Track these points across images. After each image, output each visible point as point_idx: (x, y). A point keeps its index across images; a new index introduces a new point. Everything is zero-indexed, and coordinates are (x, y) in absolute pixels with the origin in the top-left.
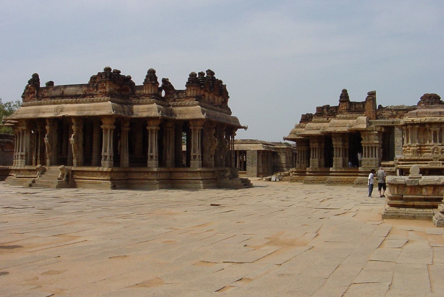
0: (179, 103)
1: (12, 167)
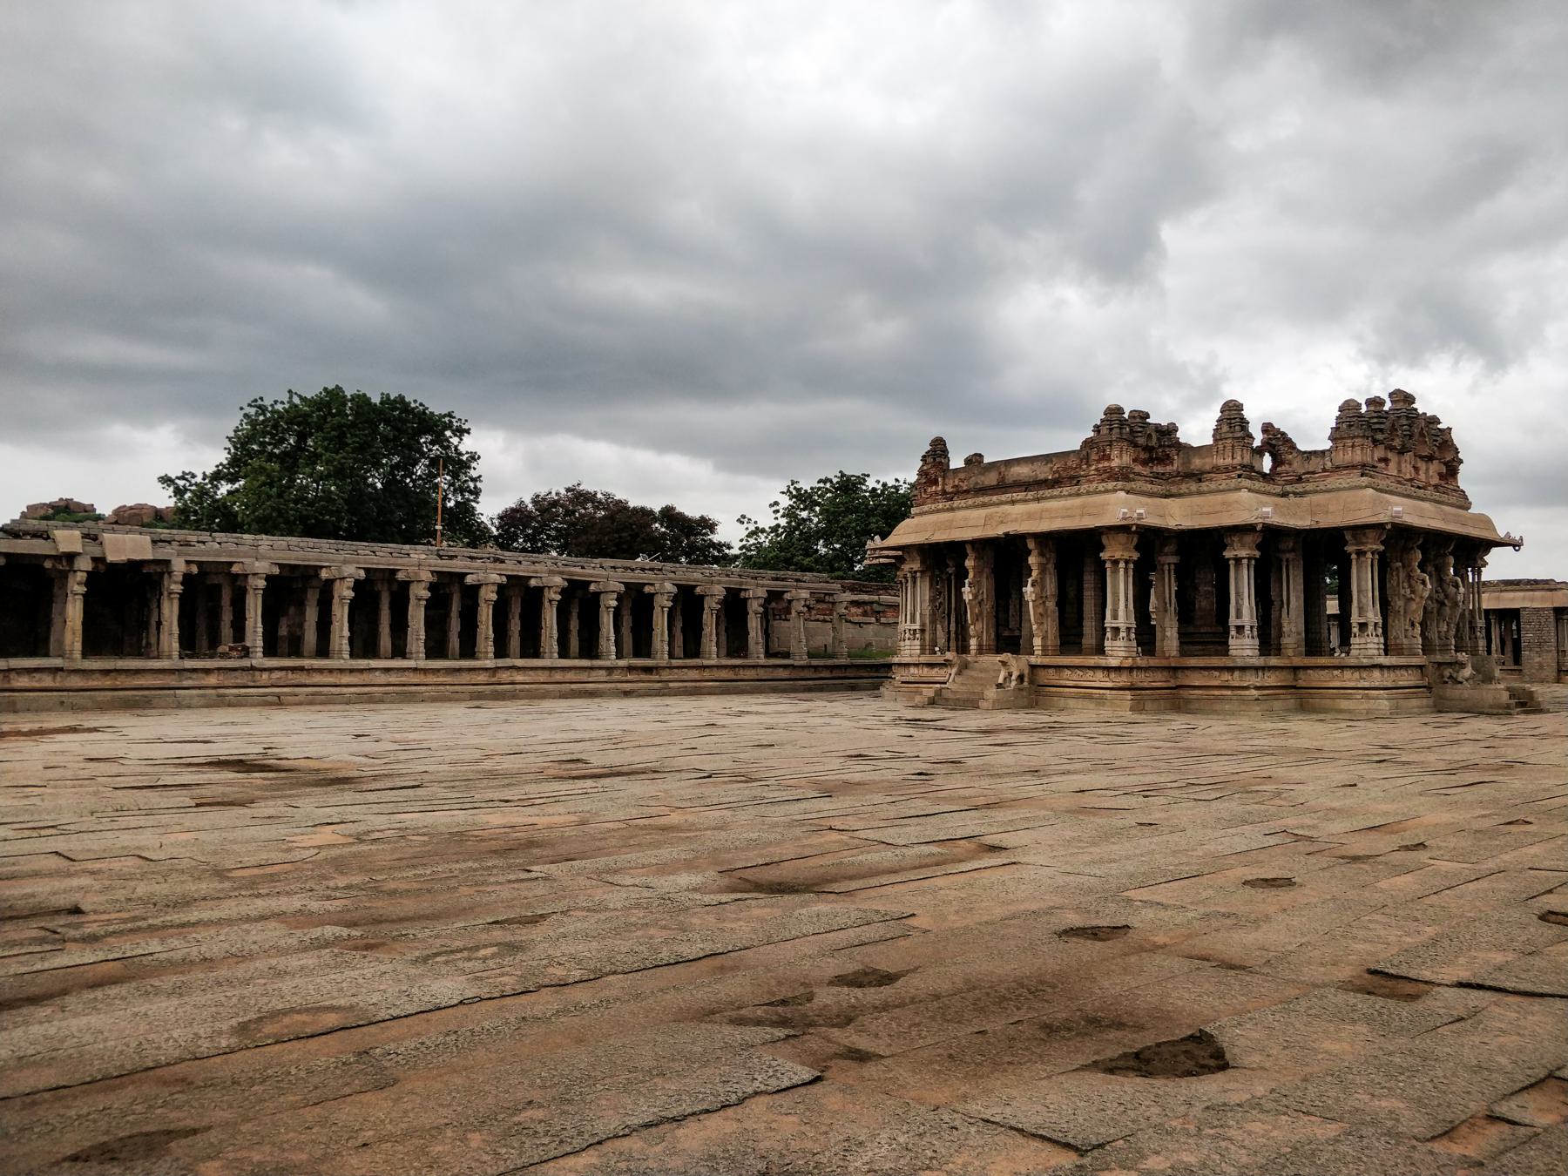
0: (1310, 487)
1: (896, 660)
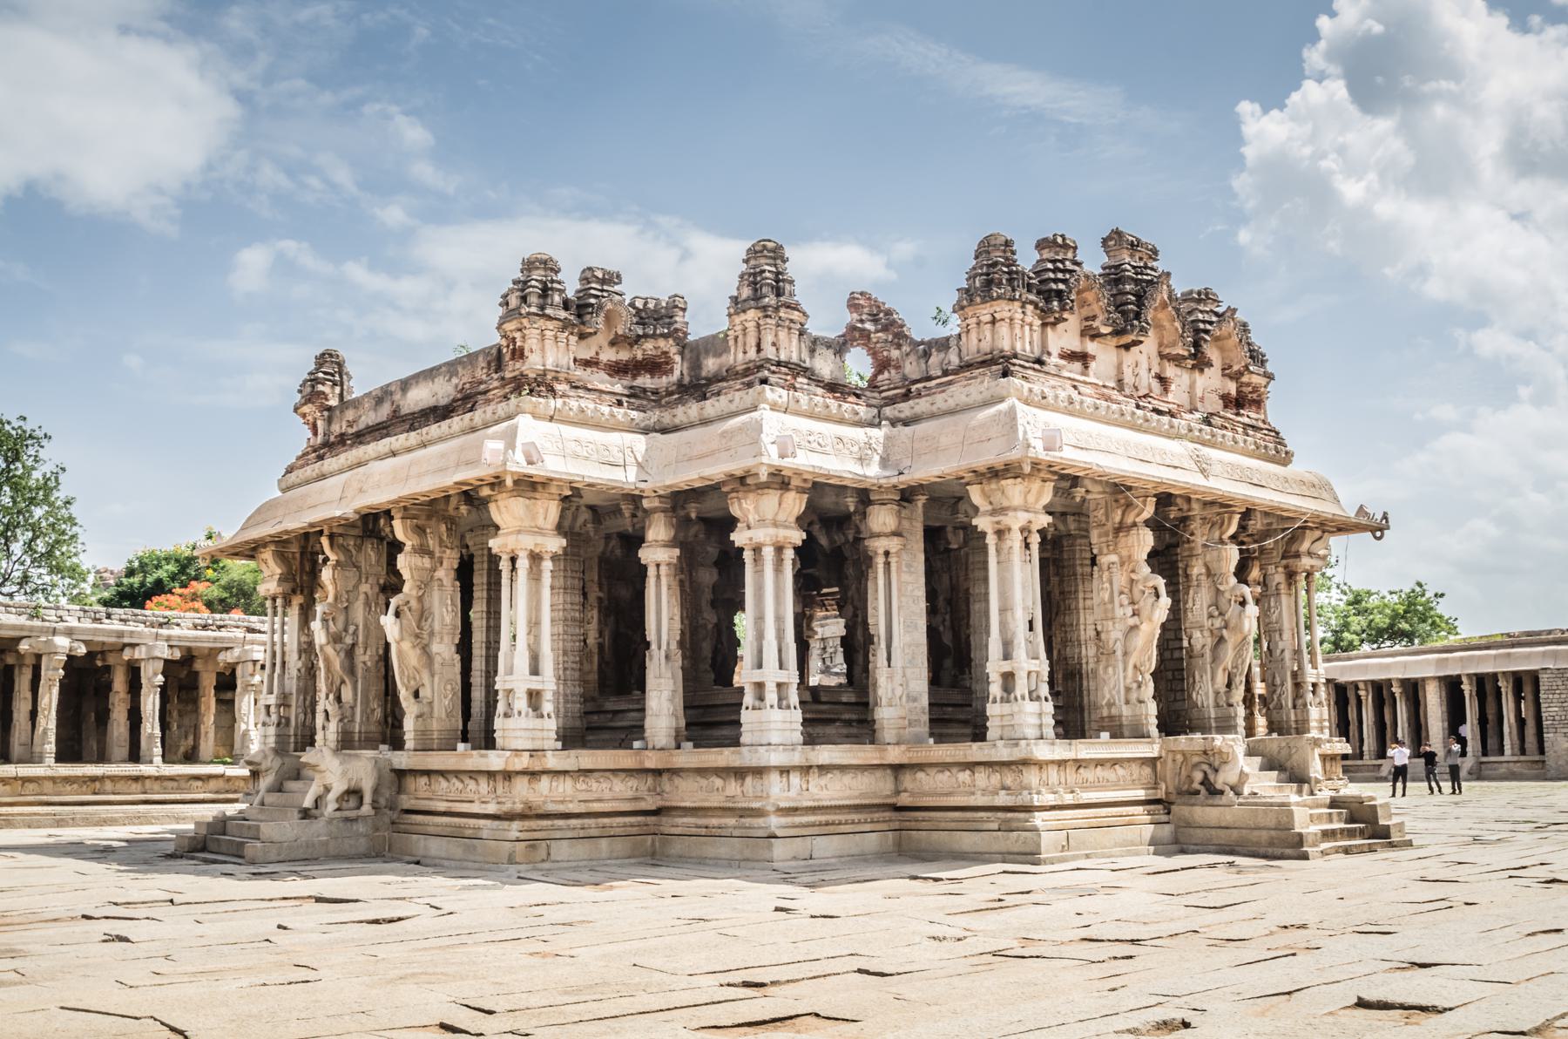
0: (921, 405)
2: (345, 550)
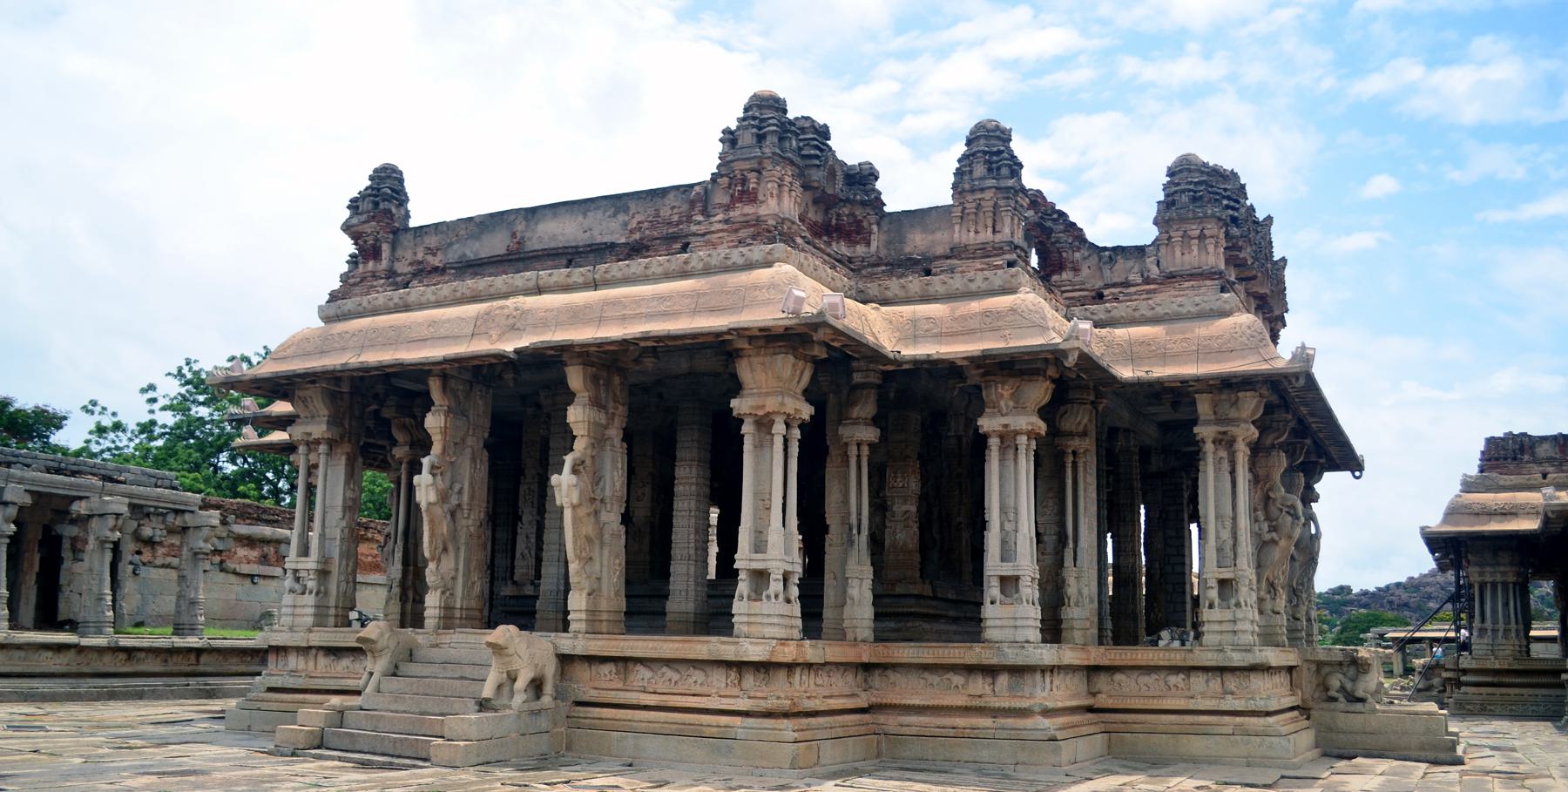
0: (1120, 310)
2: (455, 393)
